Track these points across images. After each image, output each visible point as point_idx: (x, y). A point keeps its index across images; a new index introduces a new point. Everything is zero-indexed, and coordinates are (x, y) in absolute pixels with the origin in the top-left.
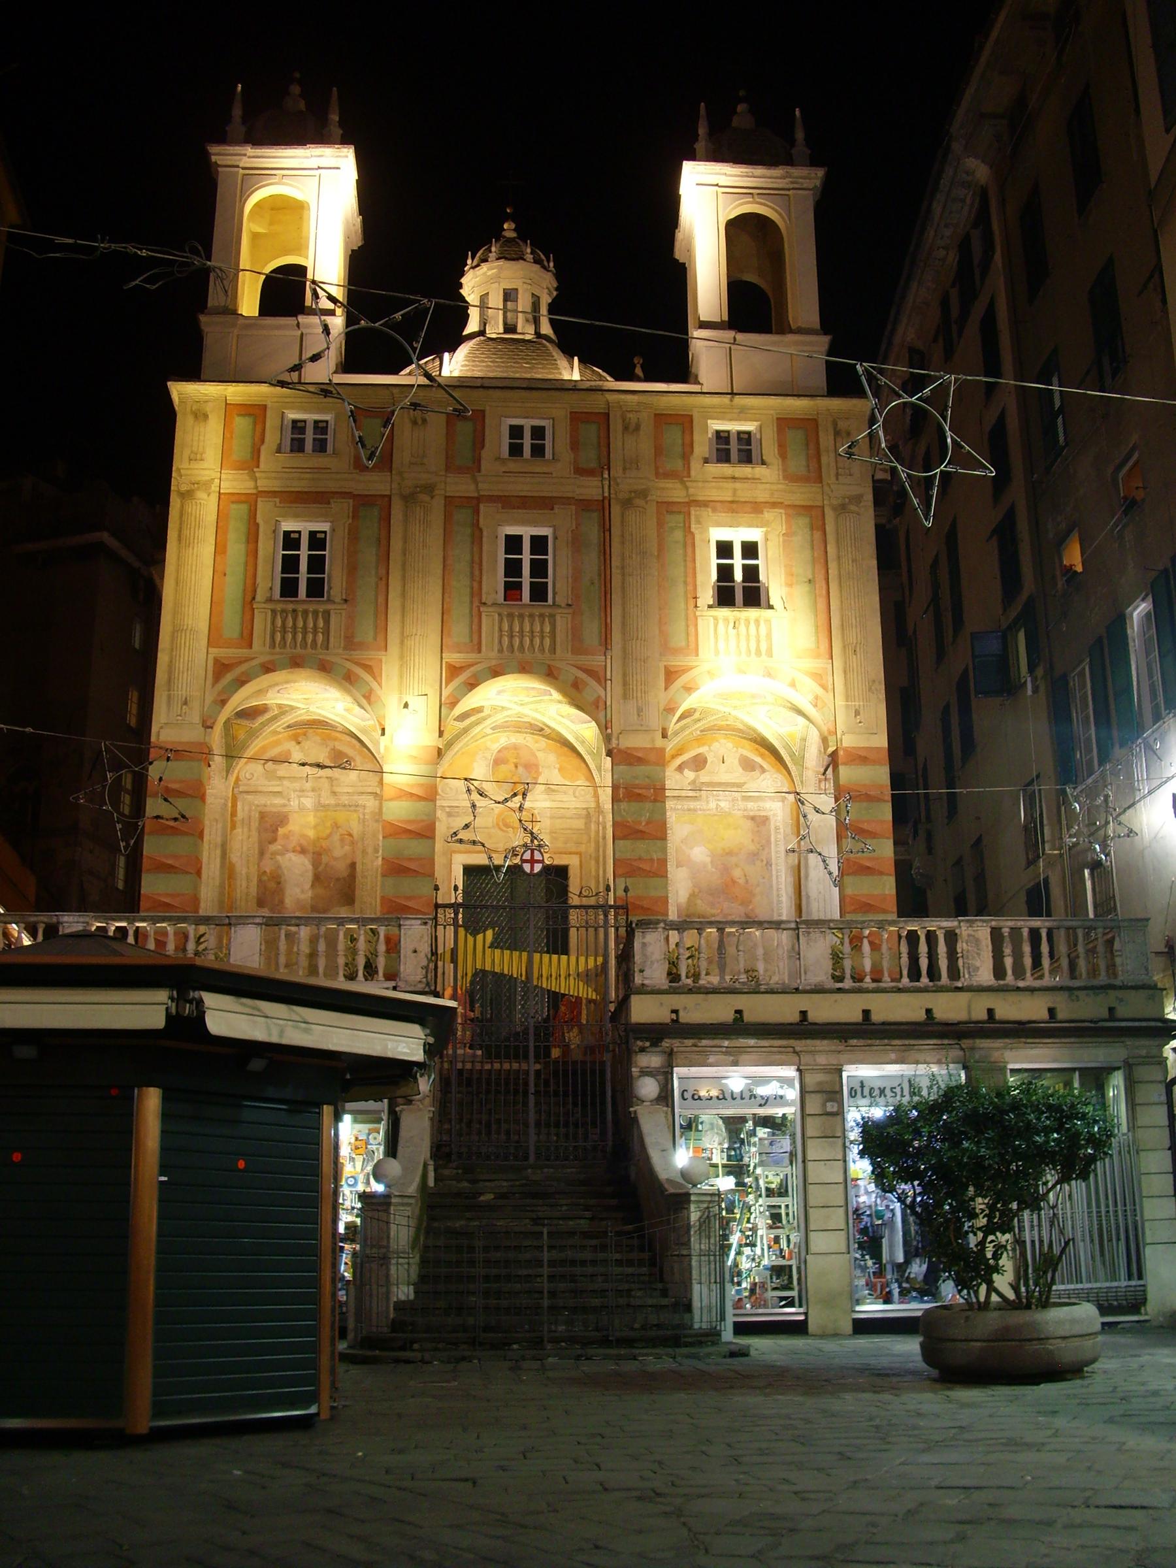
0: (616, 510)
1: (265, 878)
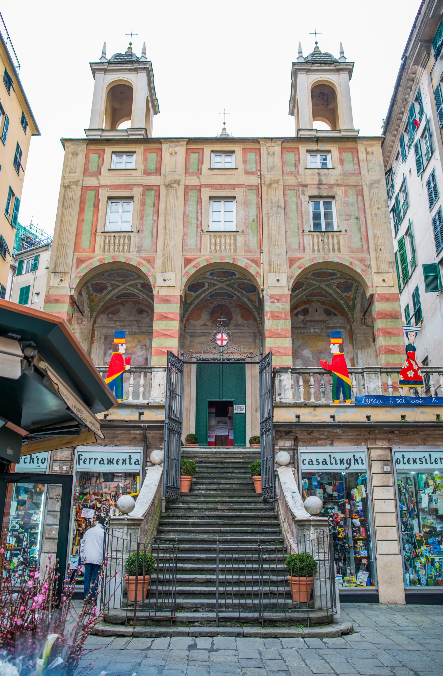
0: (264, 189)
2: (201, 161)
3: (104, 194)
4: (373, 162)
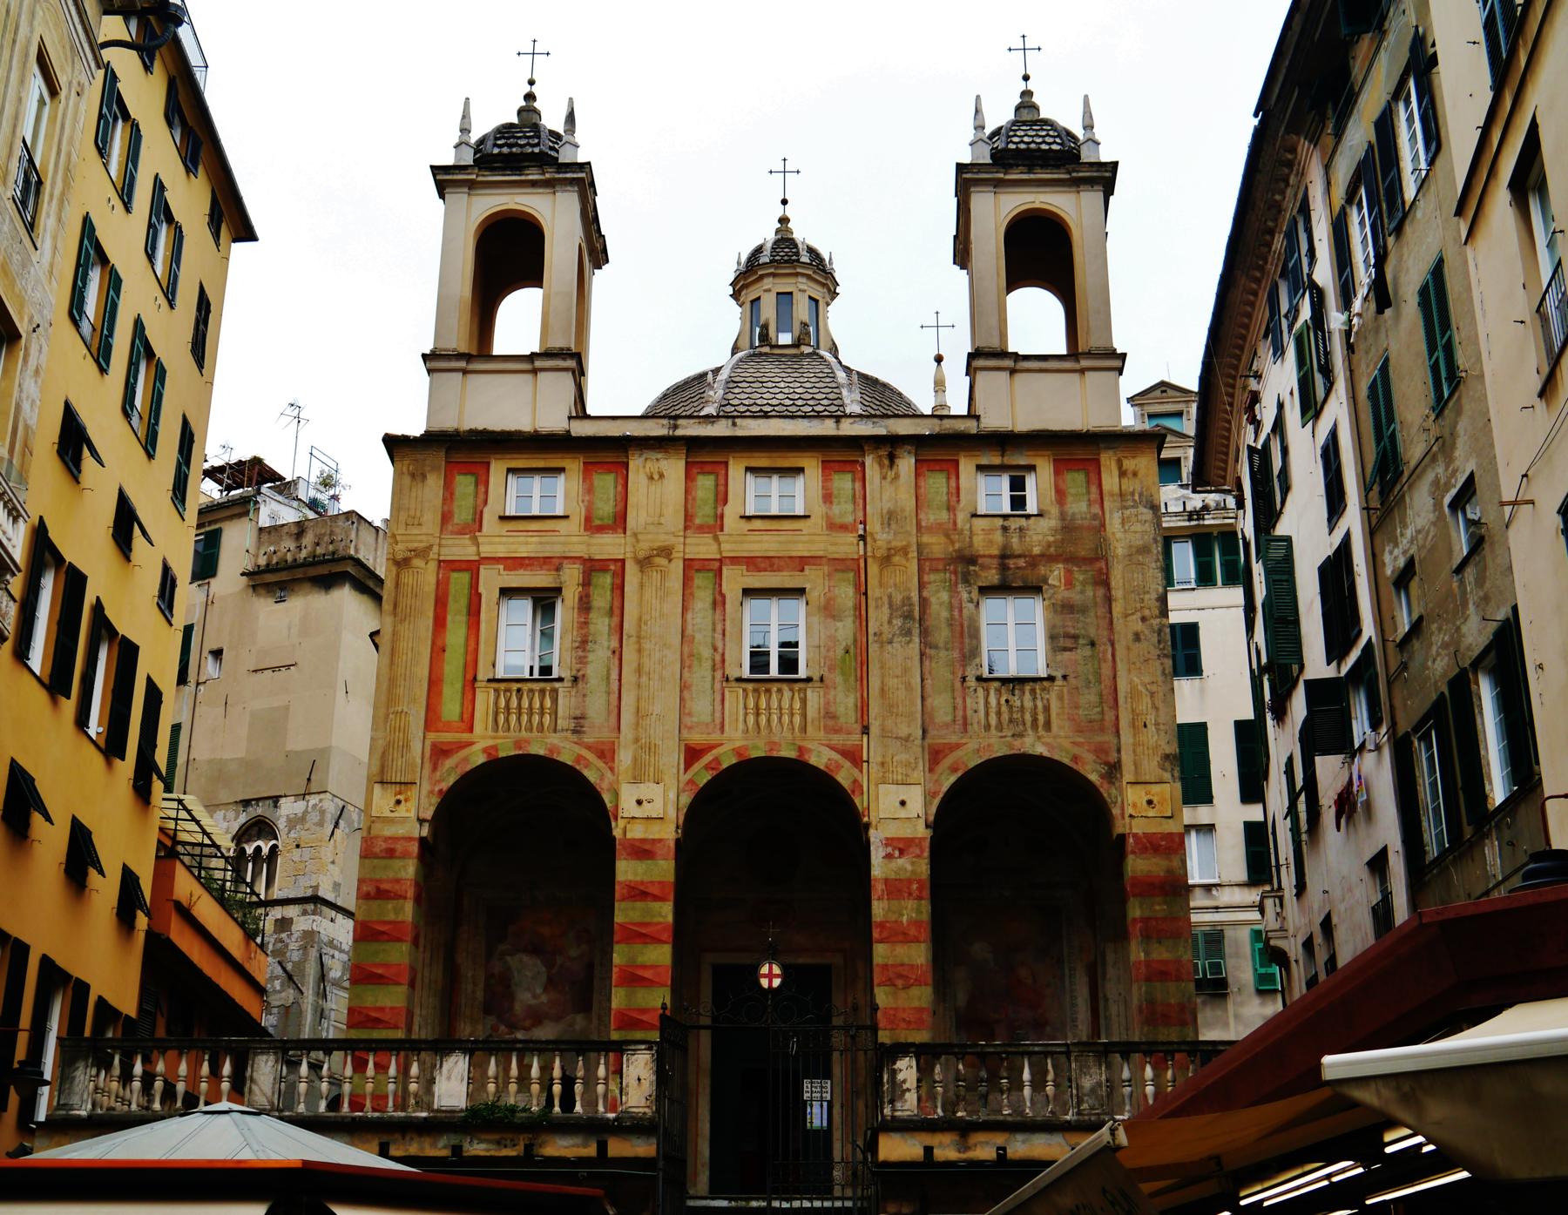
0: (873, 569)
2: (722, 498)
3: (491, 580)
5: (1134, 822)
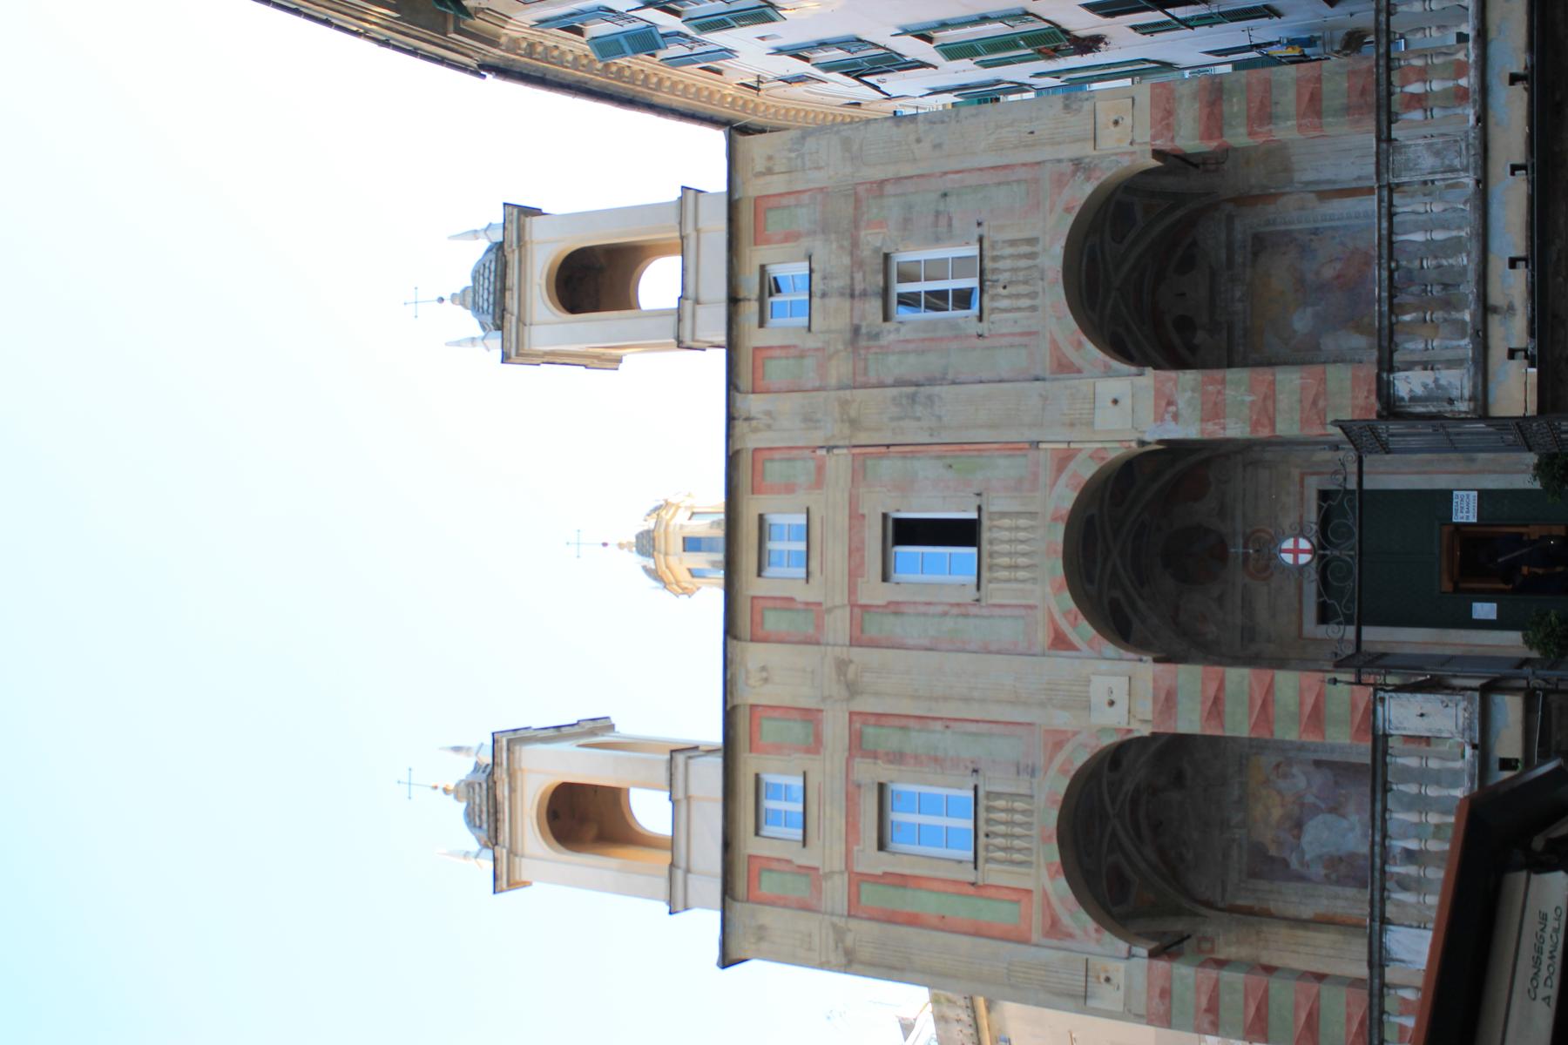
0: (863, 438)
1: (1334, 876)
3: (871, 861)
4: (793, 155)
5: (1138, 140)
